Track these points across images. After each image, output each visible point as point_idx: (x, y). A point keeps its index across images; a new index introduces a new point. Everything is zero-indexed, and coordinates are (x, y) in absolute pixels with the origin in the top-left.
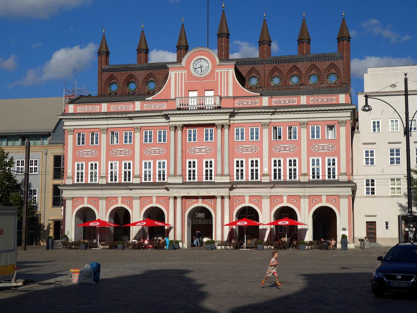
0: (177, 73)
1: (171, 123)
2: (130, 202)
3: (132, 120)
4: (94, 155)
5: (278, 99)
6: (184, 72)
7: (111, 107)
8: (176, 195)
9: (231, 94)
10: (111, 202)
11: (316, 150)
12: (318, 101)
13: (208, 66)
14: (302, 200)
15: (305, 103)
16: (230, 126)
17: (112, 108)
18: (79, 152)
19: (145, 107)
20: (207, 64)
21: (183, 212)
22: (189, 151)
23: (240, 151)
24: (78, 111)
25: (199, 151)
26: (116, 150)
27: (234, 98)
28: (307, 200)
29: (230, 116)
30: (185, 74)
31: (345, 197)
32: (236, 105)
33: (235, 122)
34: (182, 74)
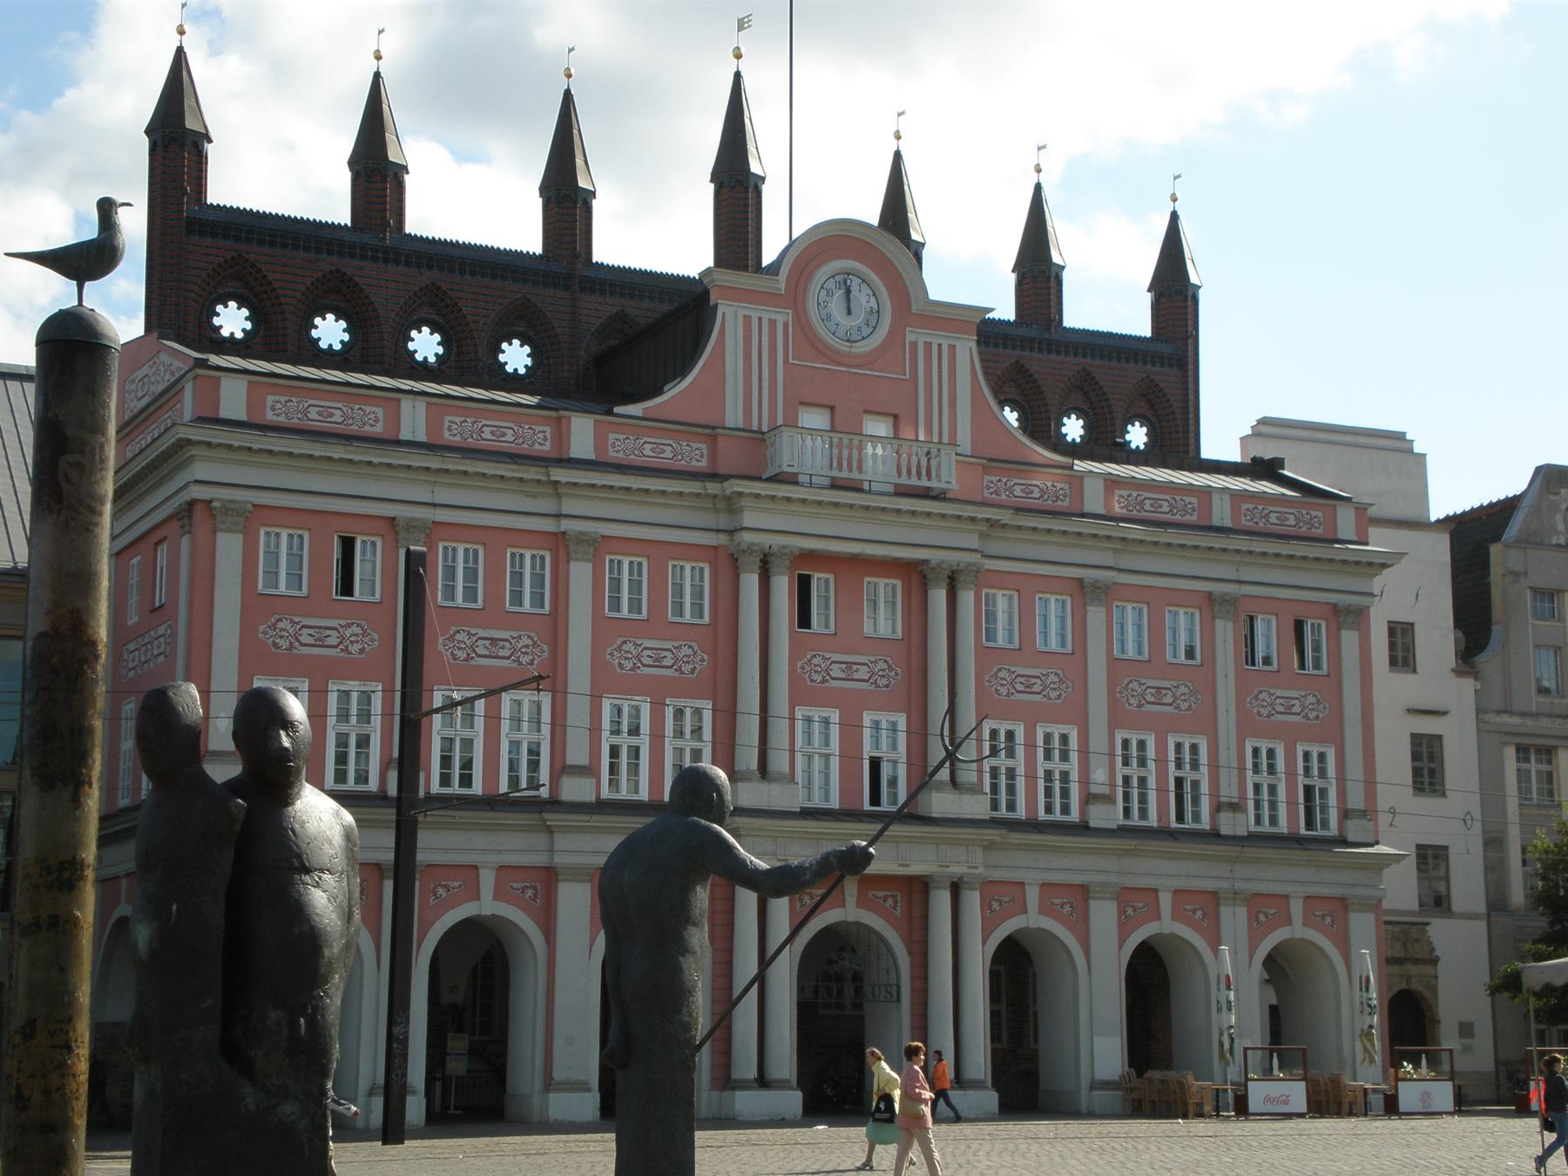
0: (755, 316)
1: (748, 537)
2: (535, 895)
4: (358, 647)
5: (1135, 494)
7: (447, 424)
10: (441, 891)
13: (875, 307)
14: (1225, 912)
17: (450, 429)
18: (274, 626)
19: (613, 445)
20: (873, 299)
22: (803, 668)
24: (270, 417)
25: (843, 675)
26: (469, 634)
28: (1242, 912)
29: (982, 536)
30: (786, 325)
34: (773, 323)
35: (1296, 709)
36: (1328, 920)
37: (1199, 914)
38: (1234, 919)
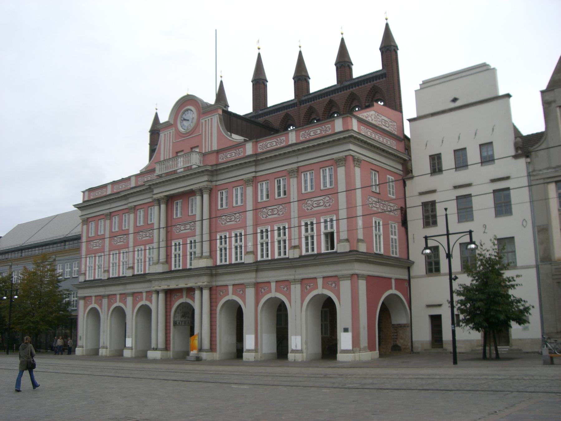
3: (128, 198)
6: (172, 131)
8: (157, 288)
9: (215, 148)
11: (309, 208)
12: (309, 134)
14: (292, 287)
15: (294, 142)
16: (211, 190)
21: (168, 310)
23: (224, 223)
27: (218, 152)
28: (298, 286)
31: (347, 277)
32: (220, 160)
33: (219, 183)
35: (322, 204)
36: (334, 285)
37: (286, 289)
38: (296, 289)
